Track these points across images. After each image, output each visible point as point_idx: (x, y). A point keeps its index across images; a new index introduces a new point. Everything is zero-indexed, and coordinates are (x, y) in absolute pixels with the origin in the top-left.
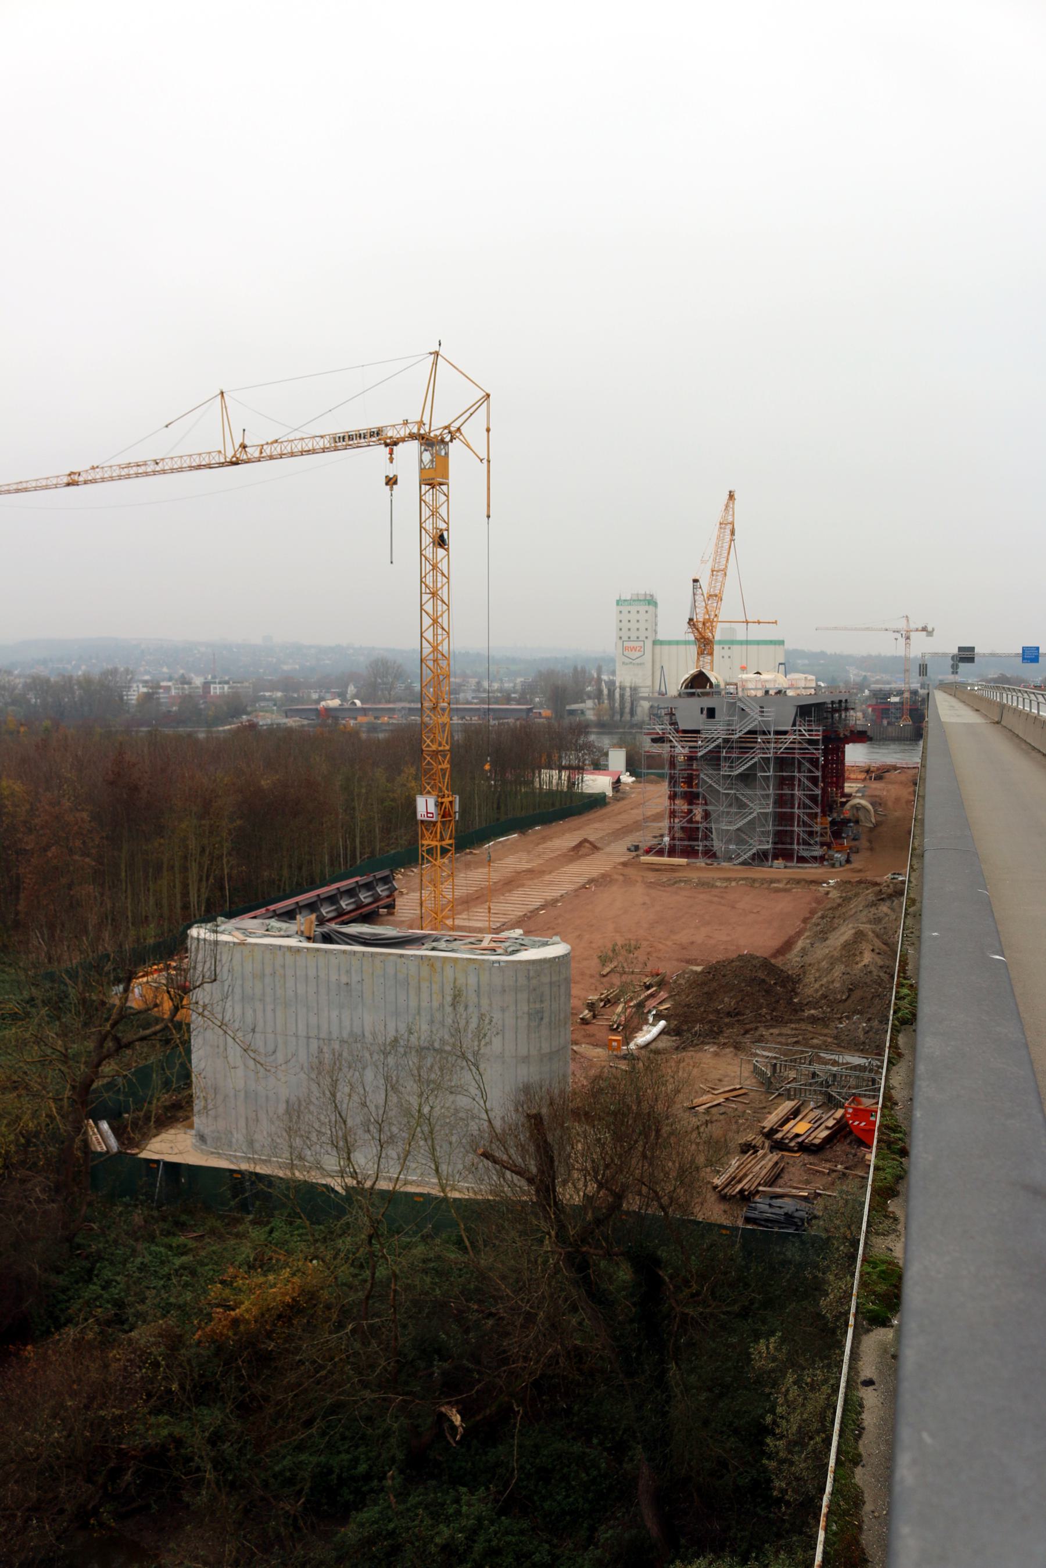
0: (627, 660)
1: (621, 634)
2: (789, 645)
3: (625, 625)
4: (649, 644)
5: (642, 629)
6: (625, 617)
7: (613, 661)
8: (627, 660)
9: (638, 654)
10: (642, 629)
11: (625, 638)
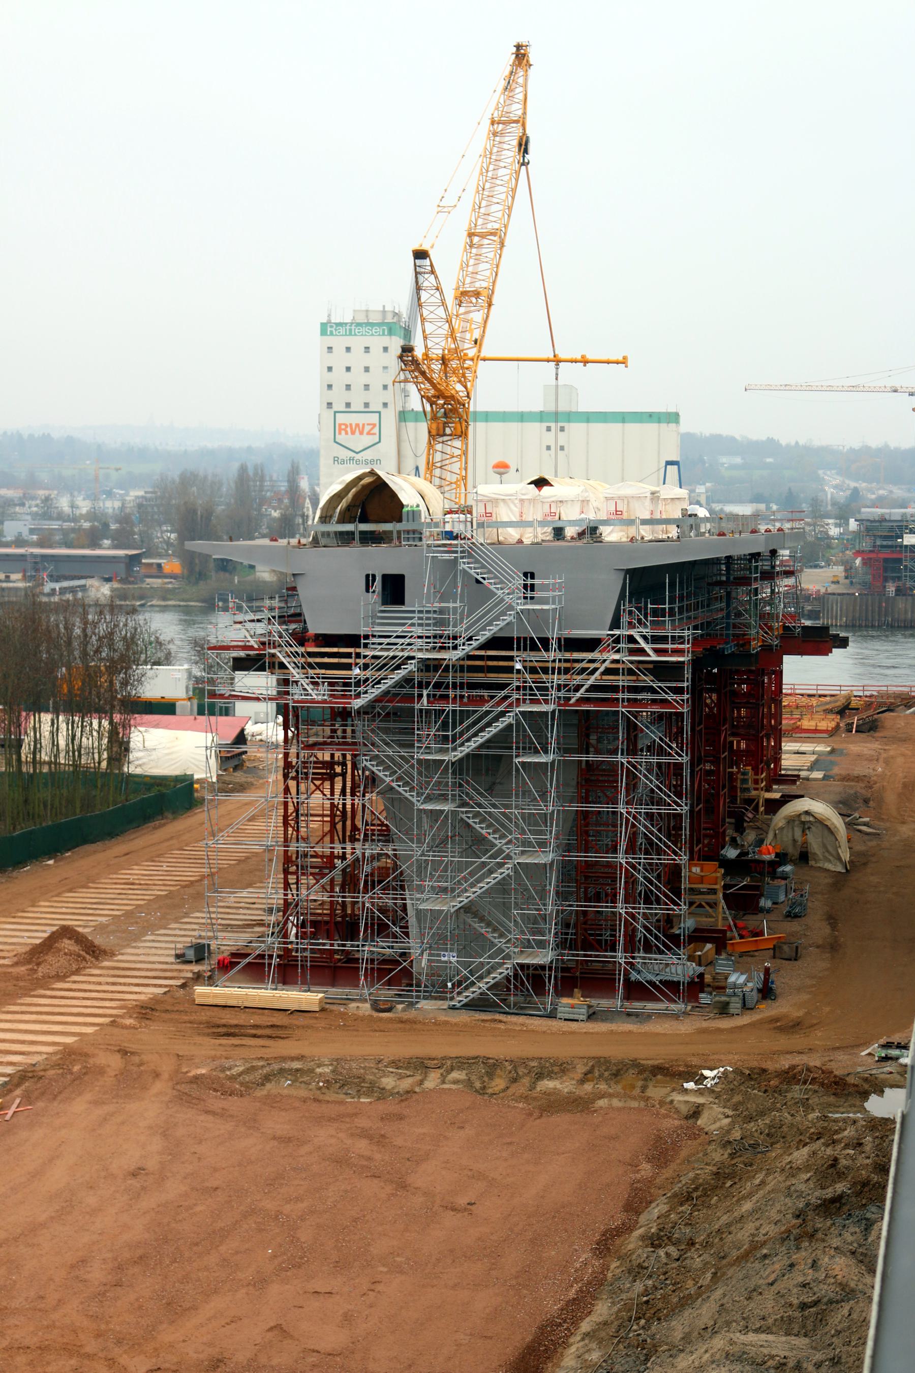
0: (344, 454)
1: (331, 396)
2: (686, 426)
3: (339, 378)
4: (390, 418)
5: (376, 386)
6: (339, 360)
7: (313, 455)
8: (344, 454)
9: (367, 440)
10: (376, 386)
11: (339, 406)
